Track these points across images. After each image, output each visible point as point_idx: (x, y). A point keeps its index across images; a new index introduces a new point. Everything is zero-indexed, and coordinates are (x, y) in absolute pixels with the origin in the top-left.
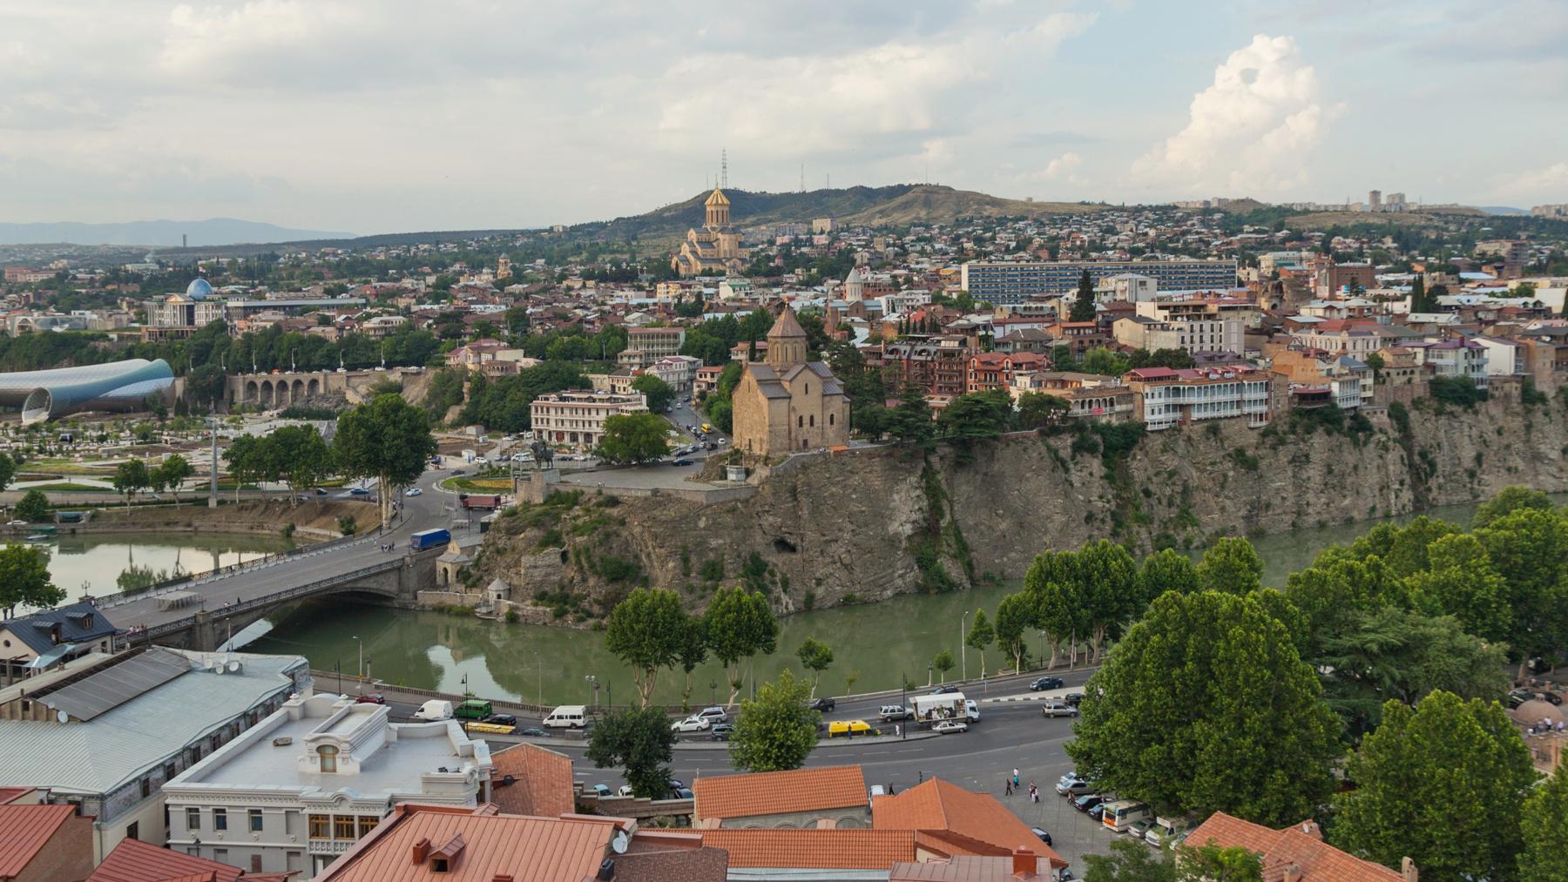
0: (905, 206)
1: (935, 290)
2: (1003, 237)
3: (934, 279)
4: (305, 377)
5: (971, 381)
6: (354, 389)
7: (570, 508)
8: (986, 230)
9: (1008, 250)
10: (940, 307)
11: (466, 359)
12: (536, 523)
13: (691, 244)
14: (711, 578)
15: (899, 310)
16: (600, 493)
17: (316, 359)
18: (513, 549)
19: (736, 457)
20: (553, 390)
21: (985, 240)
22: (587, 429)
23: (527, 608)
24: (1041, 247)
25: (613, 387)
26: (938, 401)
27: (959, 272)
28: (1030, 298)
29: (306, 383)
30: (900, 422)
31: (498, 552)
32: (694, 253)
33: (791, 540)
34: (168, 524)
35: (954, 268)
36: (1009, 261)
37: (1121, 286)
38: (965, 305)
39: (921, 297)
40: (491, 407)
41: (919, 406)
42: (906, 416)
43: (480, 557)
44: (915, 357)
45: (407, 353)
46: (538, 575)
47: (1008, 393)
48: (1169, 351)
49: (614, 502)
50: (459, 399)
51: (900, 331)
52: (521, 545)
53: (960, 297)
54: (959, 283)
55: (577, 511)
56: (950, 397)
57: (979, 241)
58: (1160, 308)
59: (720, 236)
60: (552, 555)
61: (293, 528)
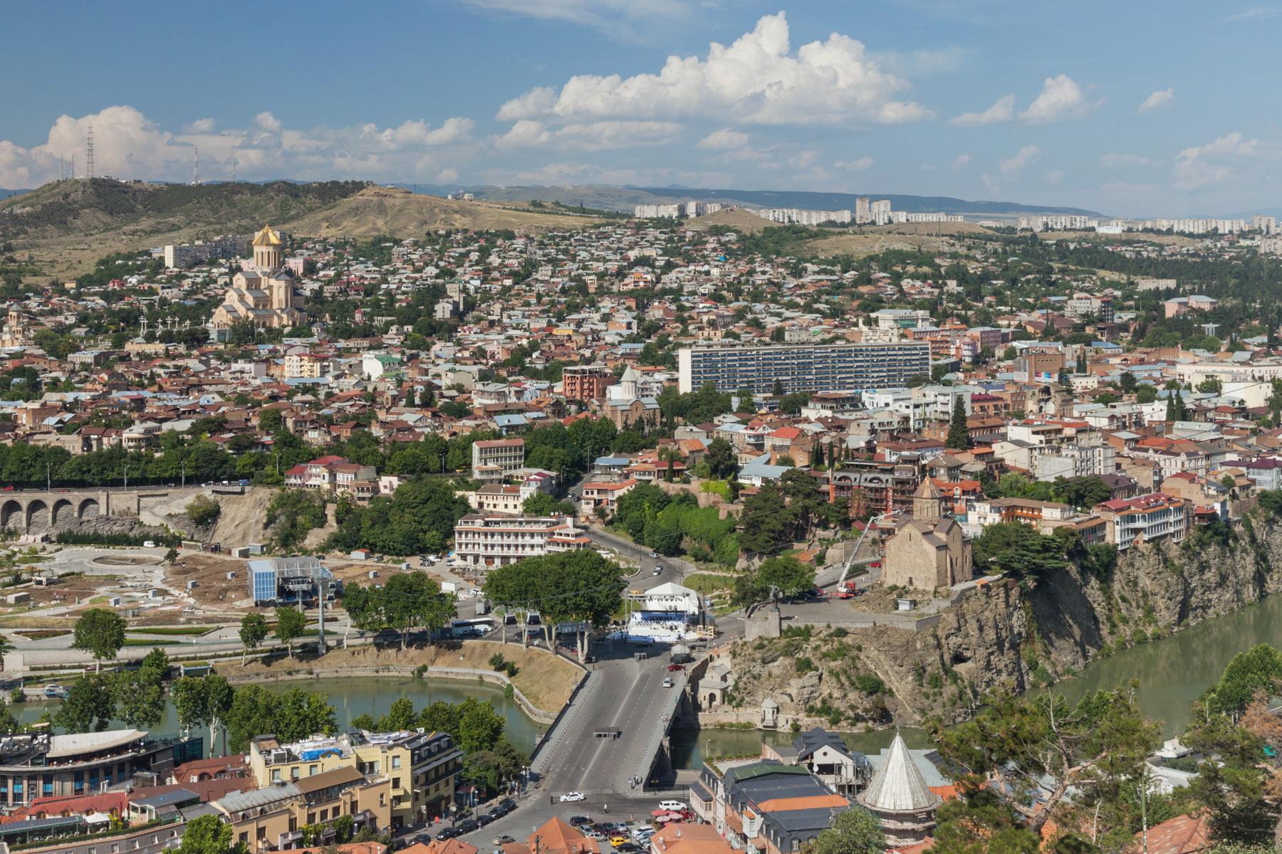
0: (356, 211)
4: (76, 496)
6: (151, 509)
7: (807, 640)
11: (317, 477)
12: (787, 652)
13: (238, 291)
16: (829, 626)
17: (64, 473)
18: (770, 675)
23: (806, 721)
25: (481, 505)
29: (76, 505)
32: (242, 298)
33: (968, 654)
34: (290, 673)
40: (377, 530)
43: (737, 683)
45: (197, 468)
46: (806, 691)
49: (842, 633)
50: (321, 521)
52: (776, 671)
55: (814, 642)
59: (273, 282)
60: (810, 678)
61: (425, 668)
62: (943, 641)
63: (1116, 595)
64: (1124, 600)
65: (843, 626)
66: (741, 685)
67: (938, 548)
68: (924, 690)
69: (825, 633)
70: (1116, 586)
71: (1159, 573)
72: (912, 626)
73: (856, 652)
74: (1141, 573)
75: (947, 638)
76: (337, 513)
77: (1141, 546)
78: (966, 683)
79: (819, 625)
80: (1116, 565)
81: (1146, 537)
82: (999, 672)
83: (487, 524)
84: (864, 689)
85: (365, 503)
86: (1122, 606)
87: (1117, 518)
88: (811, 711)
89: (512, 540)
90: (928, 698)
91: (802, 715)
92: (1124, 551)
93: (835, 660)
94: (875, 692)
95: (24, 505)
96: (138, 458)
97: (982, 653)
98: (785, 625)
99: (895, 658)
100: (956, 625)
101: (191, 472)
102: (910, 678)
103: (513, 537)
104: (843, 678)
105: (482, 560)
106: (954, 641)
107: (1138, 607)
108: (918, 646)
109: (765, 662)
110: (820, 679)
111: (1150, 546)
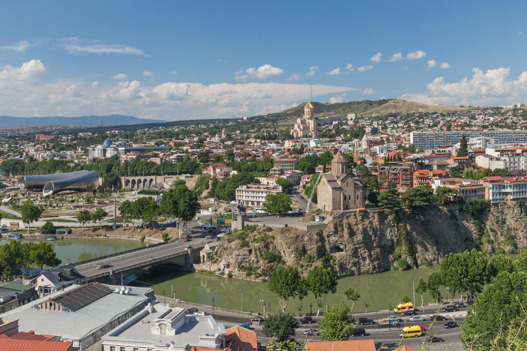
1: (399, 143)
2: (428, 121)
3: (398, 139)
5: (415, 181)
8: (420, 118)
9: (429, 127)
10: (401, 151)
14: (309, 262)
15: (385, 152)
16: (264, 226)
19: (319, 212)
20: (244, 184)
21: (419, 122)
22: (258, 200)
24: (444, 125)
25: (268, 183)
26: (401, 189)
27: (409, 136)
28: (440, 147)
30: (386, 198)
31: (224, 249)
33: (342, 247)
35: (407, 134)
36: (430, 131)
37: (479, 142)
38: (412, 149)
39: (393, 146)
41: (394, 192)
42: (388, 196)
43: (217, 251)
44: (391, 171)
47: (431, 187)
48: (500, 170)
49: (270, 229)
51: (385, 160)
52: (233, 246)
53: (410, 146)
54: (409, 140)
55: (255, 233)
56: (406, 188)
57: (417, 123)
58: (496, 151)
60: (245, 251)
62: (326, 238)
63: (488, 228)
64: (492, 230)
65: (271, 225)
66: (219, 252)
67: (333, 188)
68: (301, 263)
69: (262, 229)
70: (488, 223)
71: (521, 218)
72: (305, 229)
73: (271, 240)
74: (508, 217)
75: (328, 236)
76: (212, 184)
77: (509, 203)
78: (337, 262)
79: (260, 225)
80: (489, 211)
81: (512, 197)
82: (364, 259)
83: (248, 188)
84: (266, 259)
85: (221, 180)
86: (491, 234)
87: (491, 186)
88: (241, 268)
89: (255, 195)
90: (302, 266)
91: (236, 269)
92: (496, 205)
93: (257, 242)
94: (273, 261)
95: (142, 180)
96: (172, 165)
97: (350, 247)
98: (246, 223)
99: (287, 244)
100: (333, 230)
101: (184, 170)
102: (293, 256)
103: (261, 194)
104: (258, 252)
105: (250, 203)
106: (333, 239)
107: (502, 235)
108: (306, 239)
109: (230, 241)
110: (250, 251)
111: (514, 202)
